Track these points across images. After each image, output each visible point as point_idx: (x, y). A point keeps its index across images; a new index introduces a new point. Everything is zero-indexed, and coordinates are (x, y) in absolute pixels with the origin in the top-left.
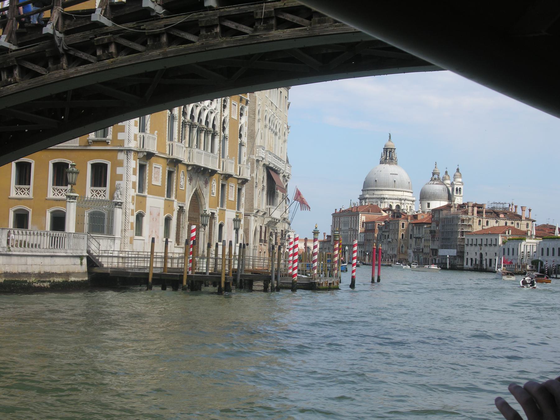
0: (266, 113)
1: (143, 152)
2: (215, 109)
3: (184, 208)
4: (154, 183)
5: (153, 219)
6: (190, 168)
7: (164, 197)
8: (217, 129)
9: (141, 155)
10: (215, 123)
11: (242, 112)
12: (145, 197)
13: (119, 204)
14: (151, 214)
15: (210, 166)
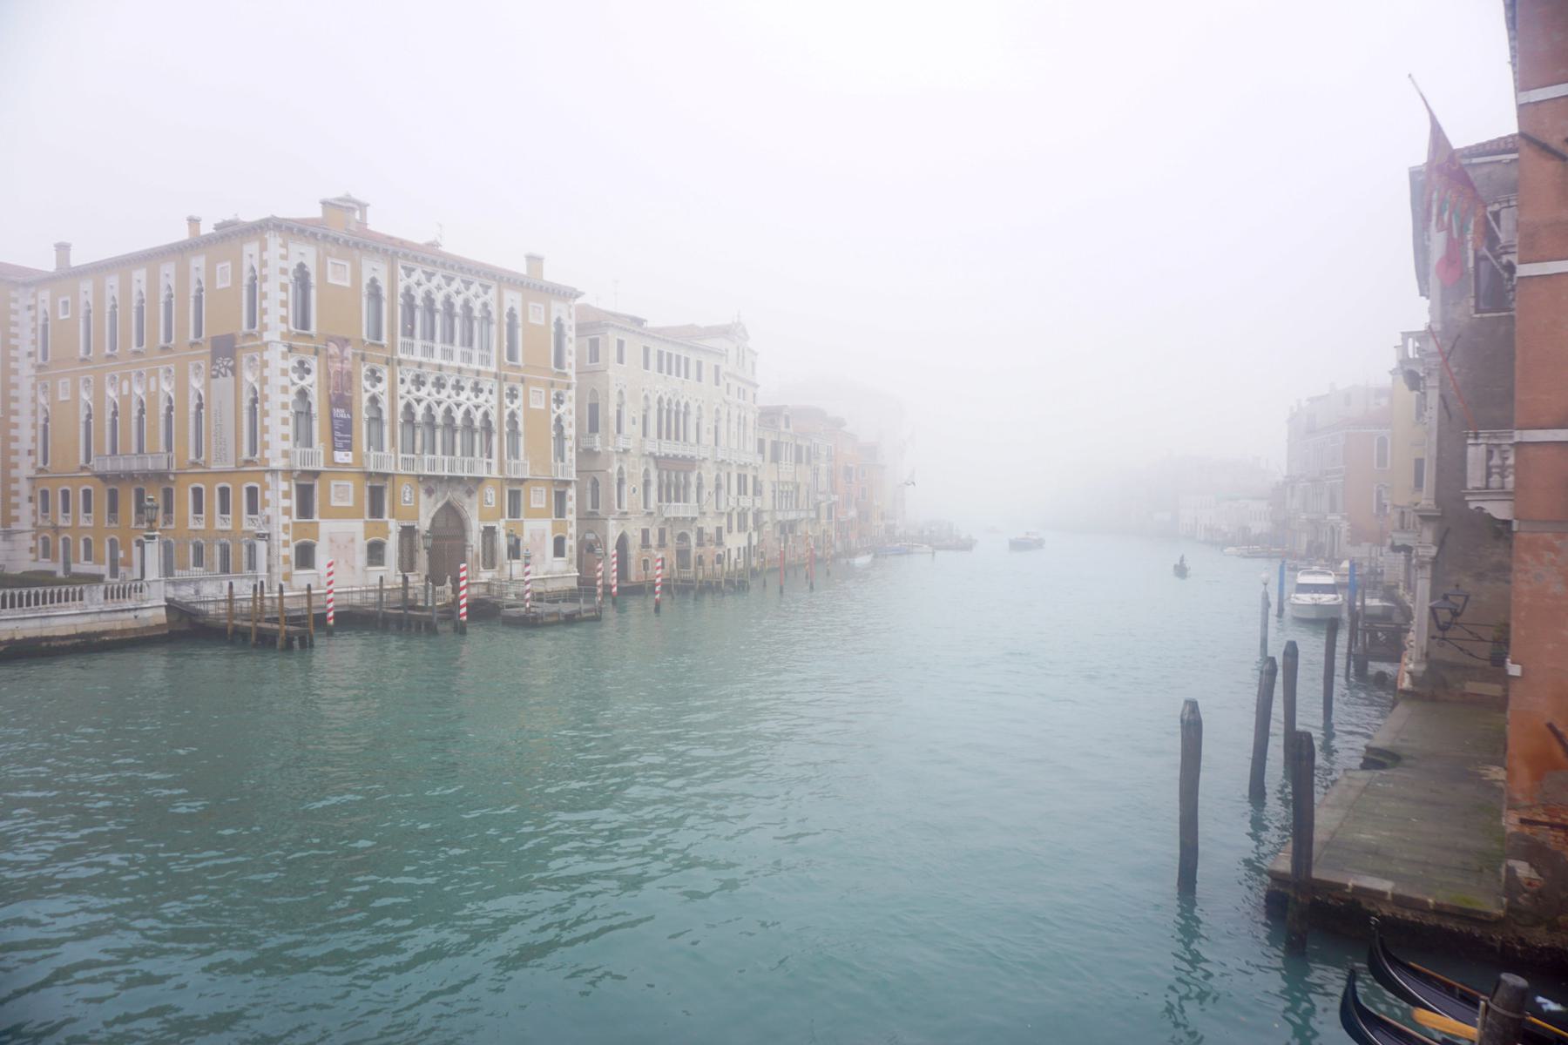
0: (645, 392)
1: (296, 471)
2: (486, 401)
3: (416, 527)
4: (335, 503)
5: (338, 547)
6: (421, 479)
7: (363, 518)
8: (495, 426)
9: (295, 474)
10: (490, 418)
11: (561, 398)
12: (317, 523)
13: (261, 536)
14: (331, 541)
15: (466, 474)
